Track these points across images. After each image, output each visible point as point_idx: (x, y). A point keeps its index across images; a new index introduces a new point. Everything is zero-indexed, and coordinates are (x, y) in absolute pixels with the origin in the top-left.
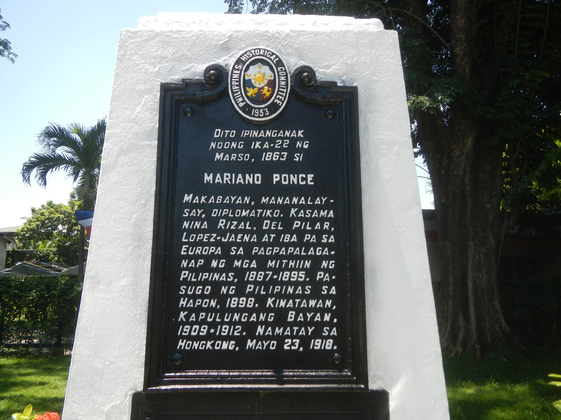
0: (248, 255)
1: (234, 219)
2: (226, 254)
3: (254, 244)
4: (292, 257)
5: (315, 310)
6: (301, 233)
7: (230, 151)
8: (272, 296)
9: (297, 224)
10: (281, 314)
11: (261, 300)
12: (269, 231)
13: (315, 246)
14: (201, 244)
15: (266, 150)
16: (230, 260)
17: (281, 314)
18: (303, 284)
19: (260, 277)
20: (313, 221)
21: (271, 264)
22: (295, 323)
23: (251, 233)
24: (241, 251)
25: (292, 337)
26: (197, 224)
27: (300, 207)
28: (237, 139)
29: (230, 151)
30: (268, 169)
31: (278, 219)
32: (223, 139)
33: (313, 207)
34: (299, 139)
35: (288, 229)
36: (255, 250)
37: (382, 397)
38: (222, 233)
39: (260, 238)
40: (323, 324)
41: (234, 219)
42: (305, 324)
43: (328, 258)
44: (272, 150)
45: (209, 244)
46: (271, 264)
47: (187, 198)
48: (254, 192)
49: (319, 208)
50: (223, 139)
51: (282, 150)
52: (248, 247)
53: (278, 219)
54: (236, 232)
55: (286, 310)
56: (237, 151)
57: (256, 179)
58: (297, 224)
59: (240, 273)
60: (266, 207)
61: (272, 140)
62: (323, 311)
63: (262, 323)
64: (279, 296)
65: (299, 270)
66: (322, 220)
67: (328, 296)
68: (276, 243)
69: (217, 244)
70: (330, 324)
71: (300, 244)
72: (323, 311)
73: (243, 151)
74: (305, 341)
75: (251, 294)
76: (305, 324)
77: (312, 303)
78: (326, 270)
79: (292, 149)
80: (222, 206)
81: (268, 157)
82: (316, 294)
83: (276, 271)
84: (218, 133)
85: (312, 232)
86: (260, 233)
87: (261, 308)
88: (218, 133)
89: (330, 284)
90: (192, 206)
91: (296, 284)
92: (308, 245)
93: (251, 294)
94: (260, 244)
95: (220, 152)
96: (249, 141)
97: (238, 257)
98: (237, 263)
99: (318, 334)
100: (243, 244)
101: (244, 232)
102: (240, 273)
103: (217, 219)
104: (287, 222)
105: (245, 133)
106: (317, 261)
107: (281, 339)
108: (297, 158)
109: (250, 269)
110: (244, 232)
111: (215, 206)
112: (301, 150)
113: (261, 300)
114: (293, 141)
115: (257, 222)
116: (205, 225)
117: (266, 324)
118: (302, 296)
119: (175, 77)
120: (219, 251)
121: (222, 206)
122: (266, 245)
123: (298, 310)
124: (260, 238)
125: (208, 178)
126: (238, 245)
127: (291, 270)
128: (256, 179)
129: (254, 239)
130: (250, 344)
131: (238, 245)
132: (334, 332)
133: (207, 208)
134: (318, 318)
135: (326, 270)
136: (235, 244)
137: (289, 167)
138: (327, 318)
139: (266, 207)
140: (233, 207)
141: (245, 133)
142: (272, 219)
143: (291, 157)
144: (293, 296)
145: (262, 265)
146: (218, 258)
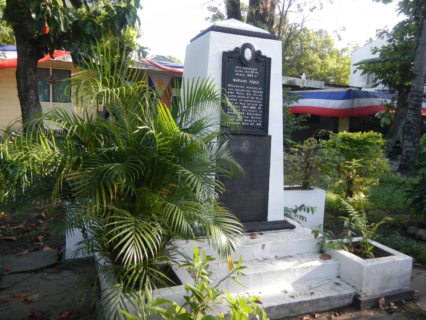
0: (243, 102)
1: (240, 92)
2: (238, 101)
3: (245, 99)
4: (253, 103)
5: (257, 116)
6: (255, 97)
7: (240, 73)
8: (248, 112)
9: (254, 94)
10: (250, 116)
11: (246, 113)
12: (248, 96)
13: (258, 100)
14: (232, 98)
15: (248, 74)
16: (239, 102)
17: (250, 116)
18: (255, 110)
19: (246, 108)
20: (258, 94)
21: (248, 104)
22: (253, 119)
23: (244, 96)
24: (241, 101)
25: (252, 122)
26: (231, 93)
27: (255, 90)
28: (242, 69)
29: (240, 73)
30: (249, 79)
31: (250, 93)
32: (238, 69)
33: (258, 90)
34: (256, 71)
35: (252, 96)
36: (245, 100)
37: (270, 137)
38: (237, 95)
39: (246, 97)
40: (259, 119)
41: (240, 92)
42: (255, 119)
43: (261, 104)
44: (250, 73)
45: (234, 98)
46: (248, 104)
47: (229, 85)
48: (245, 85)
49: (260, 91)
50: (238, 69)
51: (252, 74)
52: (243, 99)
53: (250, 93)
54: (241, 95)
55: (251, 116)
56: (241, 73)
57: (245, 81)
58: (254, 94)
59: (241, 106)
60: (248, 89)
61: (250, 71)
62: (259, 116)
63: (246, 119)
64: (250, 112)
65: (254, 106)
66: (261, 94)
67: (260, 113)
68: (250, 99)
69: (236, 98)
70: (260, 120)
71: (255, 100)
72: (259, 116)
73: (243, 73)
74: (255, 123)
75: (244, 112)
76: (255, 119)
77: (257, 115)
78: (260, 107)
79: (254, 74)
80: (237, 88)
81: (249, 75)
82: (258, 112)
83: (249, 106)
84: (237, 67)
85: (258, 97)
86: (246, 96)
87: (246, 115)
88: (237, 67)
89: (261, 110)
90: (230, 87)
91: (253, 110)
92: (257, 100)
93: (244, 112)
94: (246, 99)
95: (237, 73)
96: (244, 70)
97: (241, 102)
98: (241, 103)
99: (258, 122)
100: (242, 99)
101: (242, 95)
102: (241, 106)
103: (237, 91)
104: (252, 93)
105: (243, 68)
106: (258, 104)
107: (250, 123)
108: (256, 76)
109: (243, 105)
110: (242, 95)
111: (236, 88)
112: (256, 74)
113: (246, 113)
114: (255, 71)
115: (245, 93)
116: (233, 93)
117: (247, 119)
118: (255, 113)
119: (227, 50)
120: (236, 100)
121: (237, 88)
122: (247, 99)
123: (254, 116)
124: (246, 97)
125: (234, 80)
126: (241, 99)
127: (253, 106)
128: (245, 81)
129: (245, 98)
130: (243, 123)
131: (241, 99)
132: (261, 122)
133: (234, 88)
134: (258, 118)
135: (260, 107)
136: (240, 98)
137: (254, 79)
138: (260, 118)
139: (248, 89)
140: (240, 88)
141: (243, 68)
142: (249, 93)
143: (254, 76)
144: (253, 113)
145: (246, 105)
146: (236, 102)
